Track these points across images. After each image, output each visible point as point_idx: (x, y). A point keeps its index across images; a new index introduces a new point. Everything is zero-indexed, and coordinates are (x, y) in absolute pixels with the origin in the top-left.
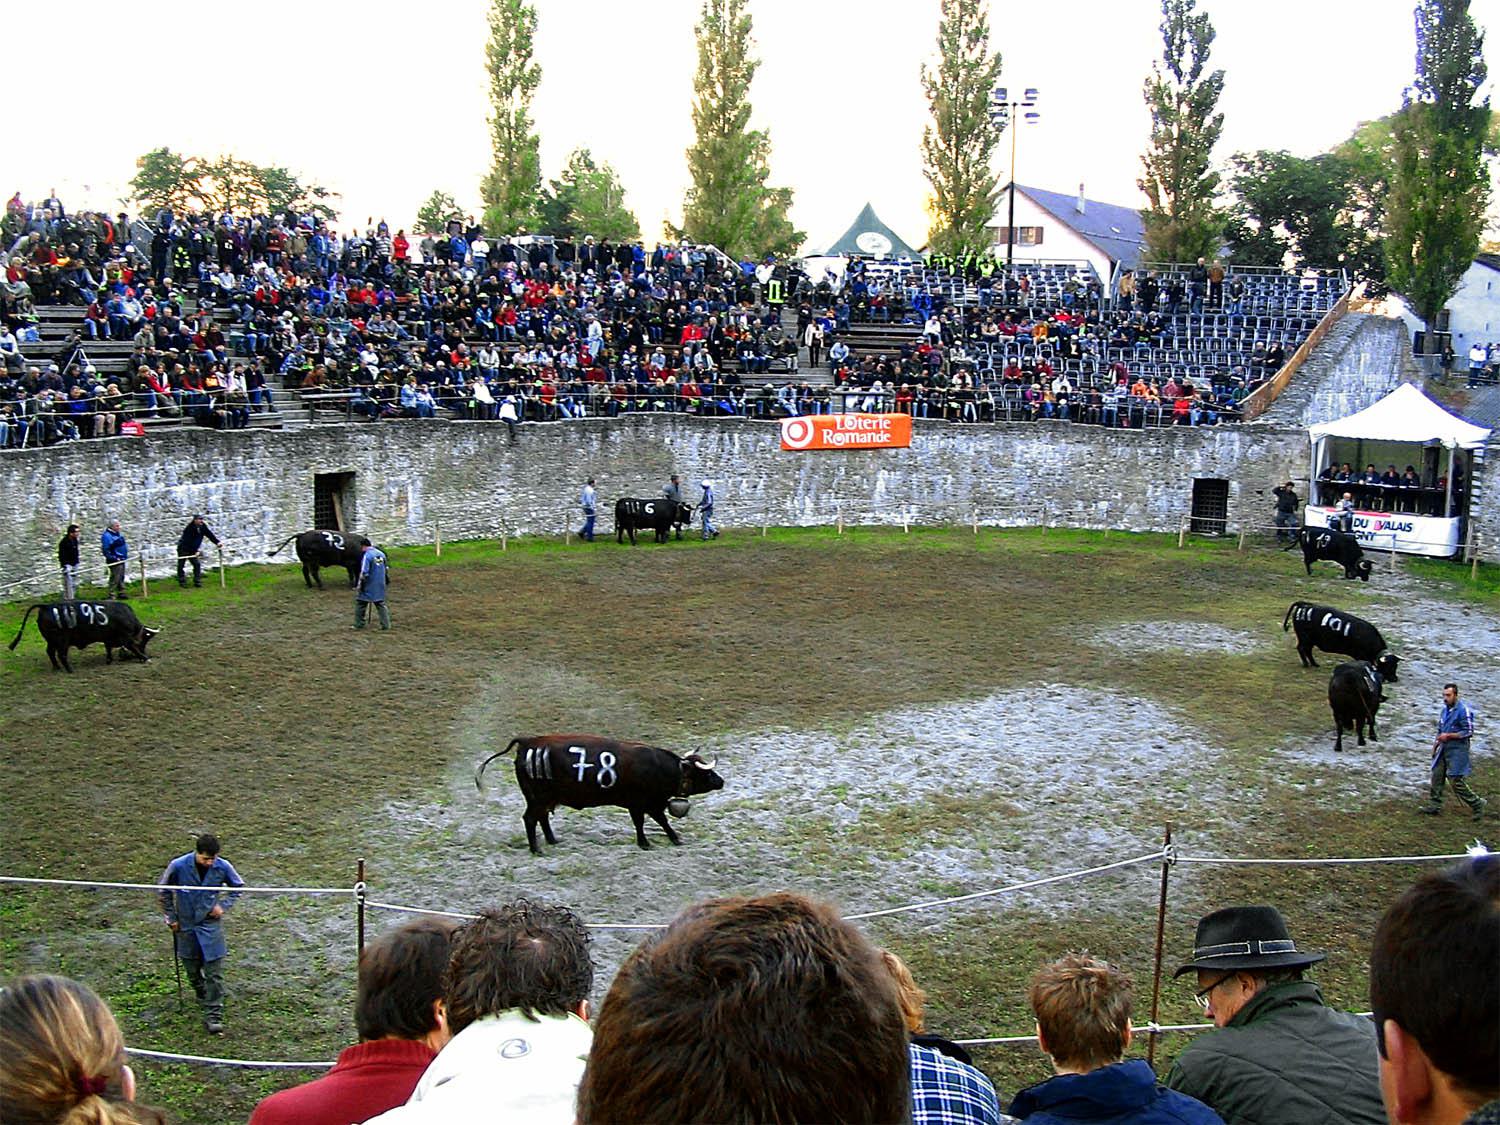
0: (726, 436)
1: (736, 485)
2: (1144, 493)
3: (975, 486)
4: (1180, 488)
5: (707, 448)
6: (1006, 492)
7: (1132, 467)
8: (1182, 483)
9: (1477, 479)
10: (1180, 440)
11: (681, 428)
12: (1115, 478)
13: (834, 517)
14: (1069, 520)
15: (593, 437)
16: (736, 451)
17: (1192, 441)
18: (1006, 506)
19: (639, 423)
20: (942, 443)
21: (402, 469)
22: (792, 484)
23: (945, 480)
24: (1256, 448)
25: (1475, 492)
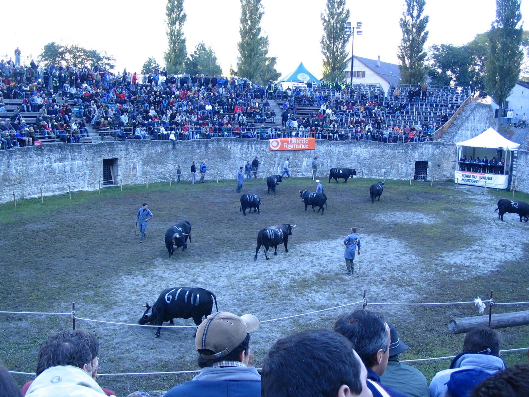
5: (243, 150)
15: (203, 146)
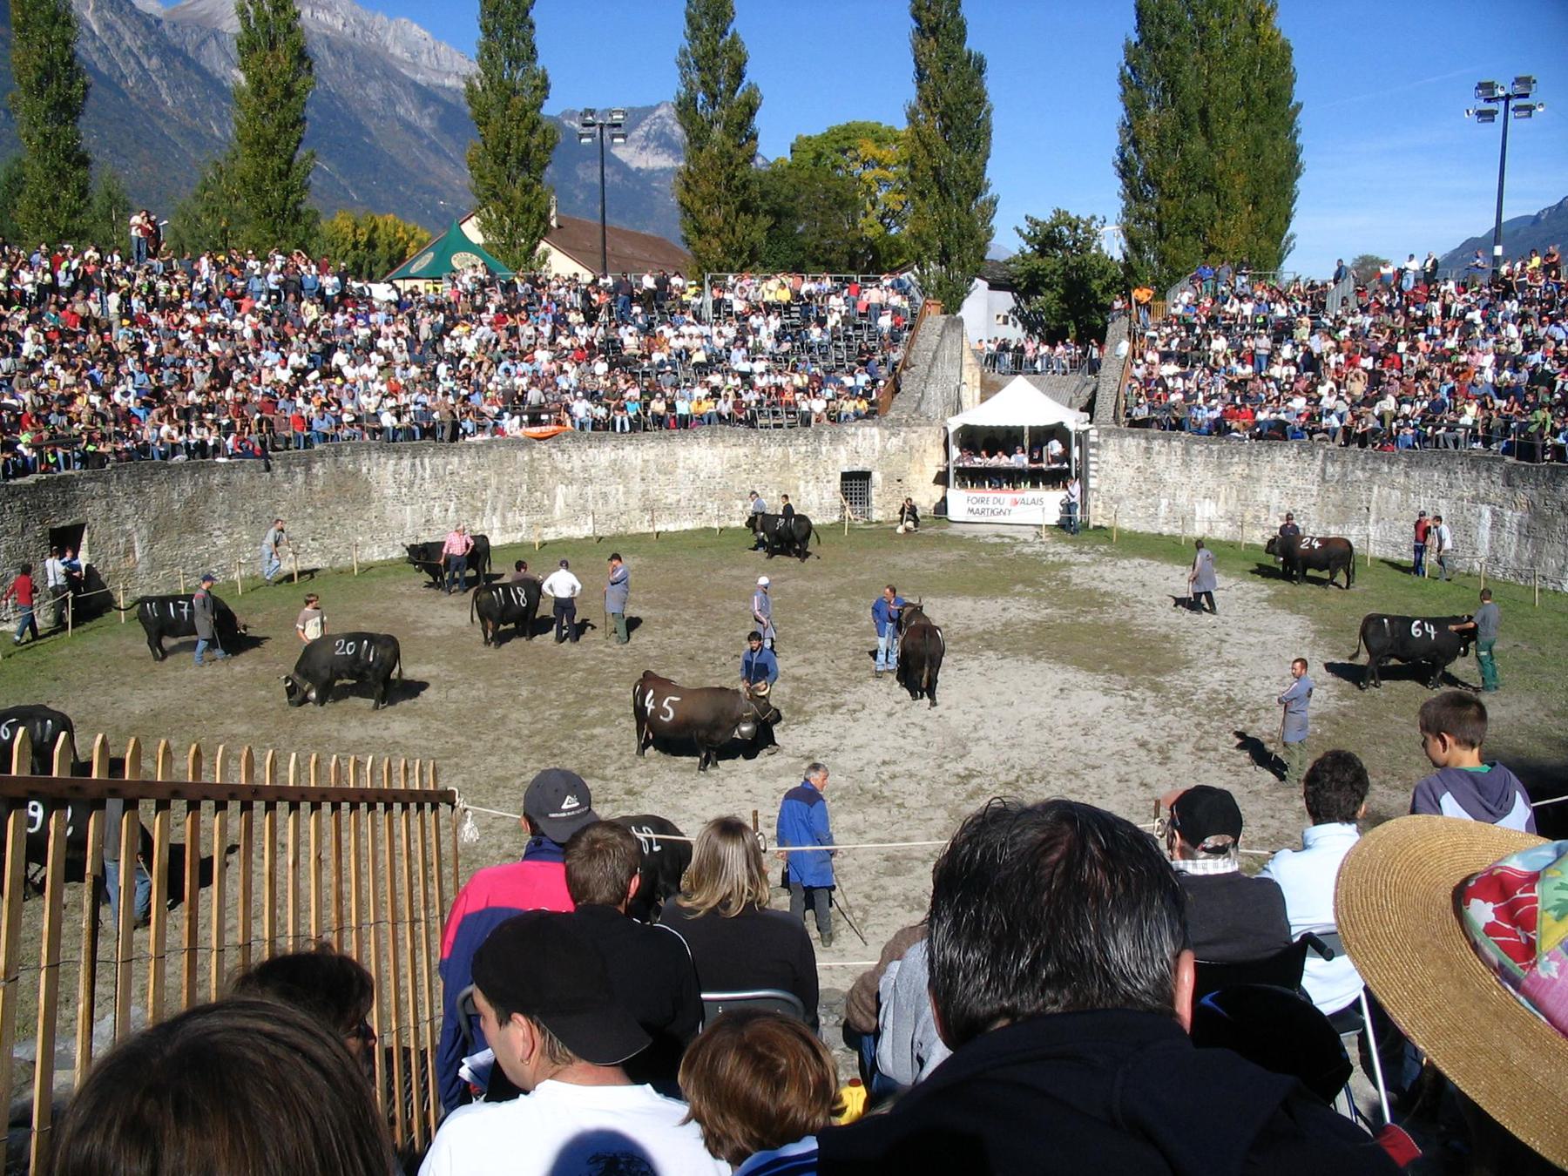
0: (418, 462)
1: (429, 510)
2: (797, 488)
3: (645, 493)
4: (828, 482)
6: (672, 498)
7: (785, 465)
8: (831, 477)
9: (1094, 455)
10: (826, 436)
11: (376, 456)
12: (769, 476)
13: (520, 535)
14: (730, 519)
16: (427, 476)
17: (836, 439)
18: (672, 510)
19: (338, 453)
20: (613, 454)
21: (127, 517)
22: (480, 505)
23: (617, 490)
24: (893, 440)
25: (1092, 466)
